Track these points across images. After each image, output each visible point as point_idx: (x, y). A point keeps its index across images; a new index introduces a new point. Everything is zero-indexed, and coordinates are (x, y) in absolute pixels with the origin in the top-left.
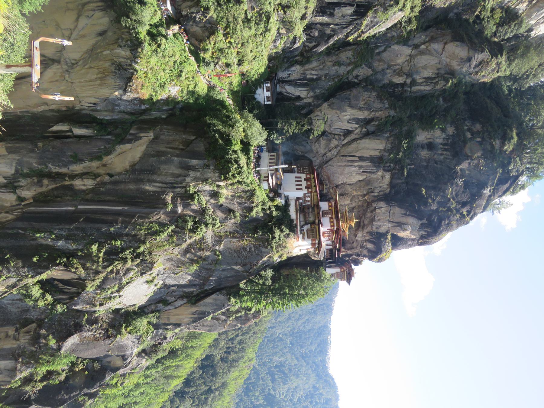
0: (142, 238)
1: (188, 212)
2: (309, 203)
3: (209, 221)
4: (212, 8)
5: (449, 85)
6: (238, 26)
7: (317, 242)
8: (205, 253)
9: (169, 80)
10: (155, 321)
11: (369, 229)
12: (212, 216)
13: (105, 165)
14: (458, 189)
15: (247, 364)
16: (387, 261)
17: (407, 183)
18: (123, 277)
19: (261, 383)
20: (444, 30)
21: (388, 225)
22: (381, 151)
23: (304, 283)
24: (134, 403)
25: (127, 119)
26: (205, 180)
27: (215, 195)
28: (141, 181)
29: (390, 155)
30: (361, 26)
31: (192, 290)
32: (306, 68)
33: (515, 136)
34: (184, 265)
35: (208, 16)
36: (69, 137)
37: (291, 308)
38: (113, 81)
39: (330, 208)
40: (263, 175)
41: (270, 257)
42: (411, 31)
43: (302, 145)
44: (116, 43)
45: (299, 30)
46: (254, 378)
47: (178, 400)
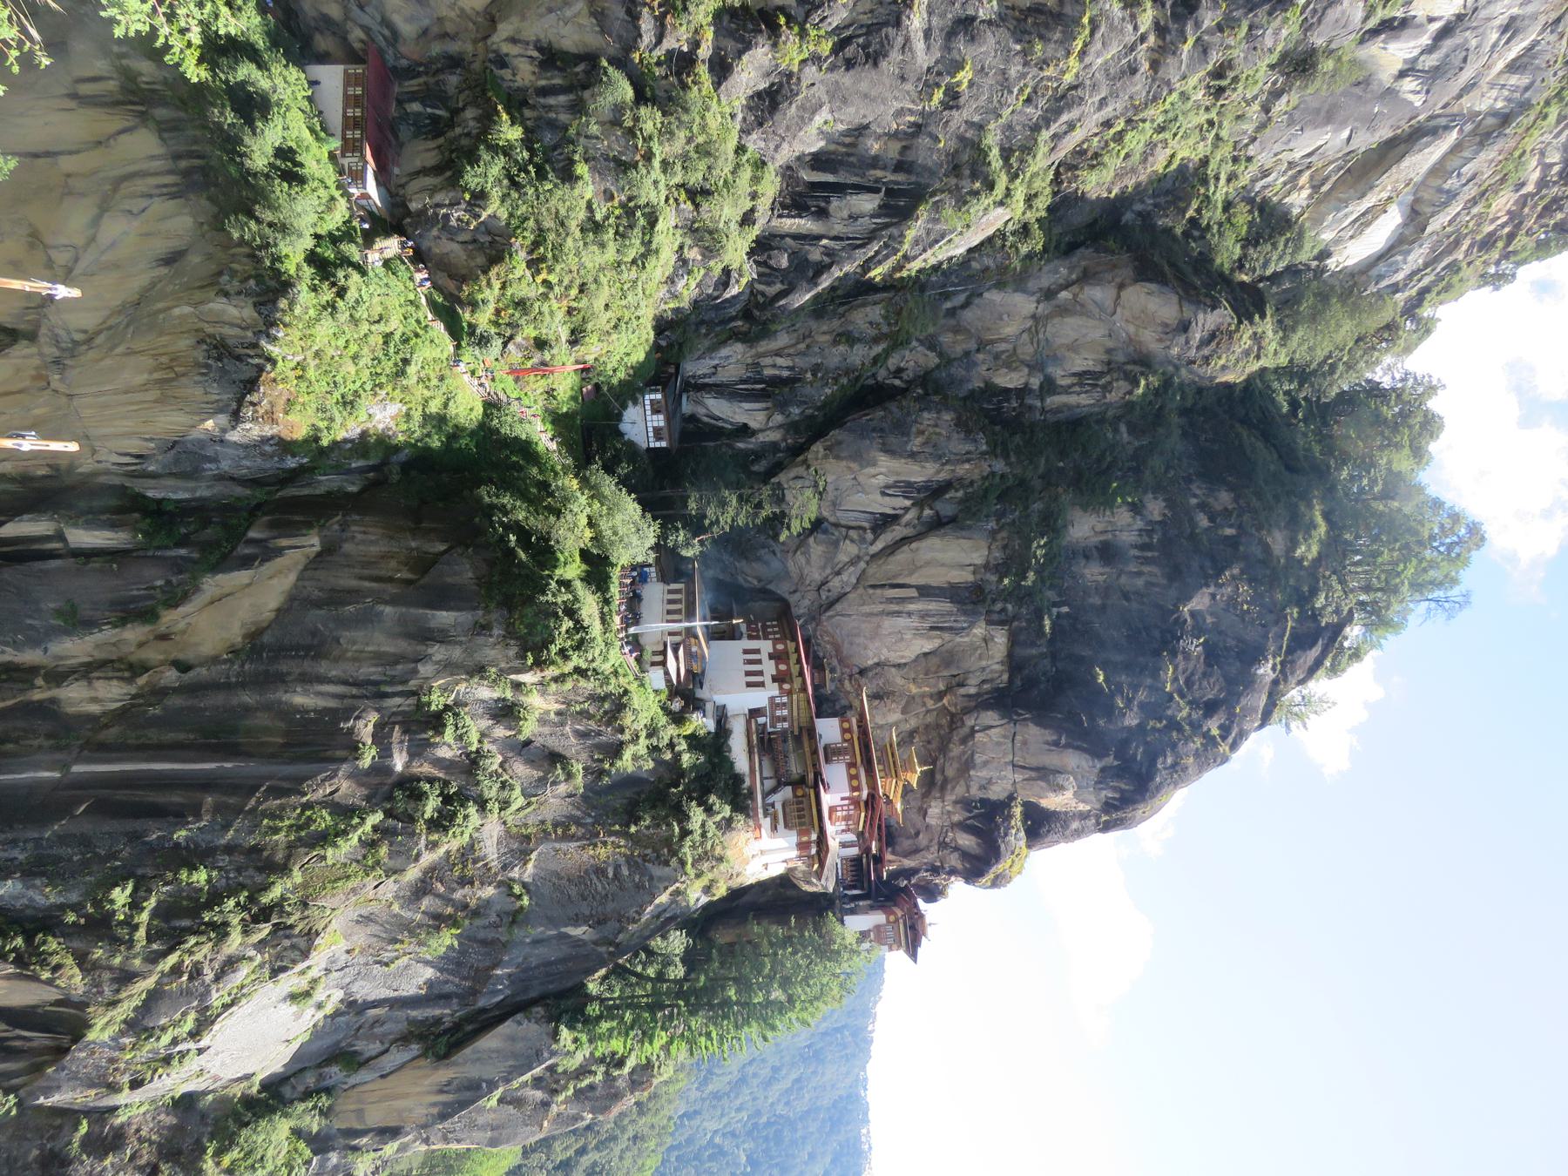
0: (280, 856)
1: (427, 769)
2: (786, 725)
3: (491, 791)
4: (495, 194)
5: (1141, 391)
6: (569, 241)
7: (814, 837)
8: (479, 893)
9: (368, 387)
10: (314, 1124)
11: (960, 790)
12: (499, 776)
13: (164, 637)
16: (1017, 880)
17: (1054, 656)
18: (214, 987)
20: (1113, 253)
22: (976, 569)
23: (783, 965)
25: (238, 499)
26: (479, 671)
27: (506, 712)
28: (281, 679)
29: (1001, 580)
30: (901, 243)
31: (437, 1012)
32: (760, 350)
33: (1319, 520)
34: (412, 933)
35: (484, 215)
36: (52, 555)
37: (746, 1048)
38: (199, 391)
39: (848, 736)
40: (649, 649)
41: (678, 892)
42: (1030, 256)
43: (759, 559)
44: (213, 283)
45: (736, 251)
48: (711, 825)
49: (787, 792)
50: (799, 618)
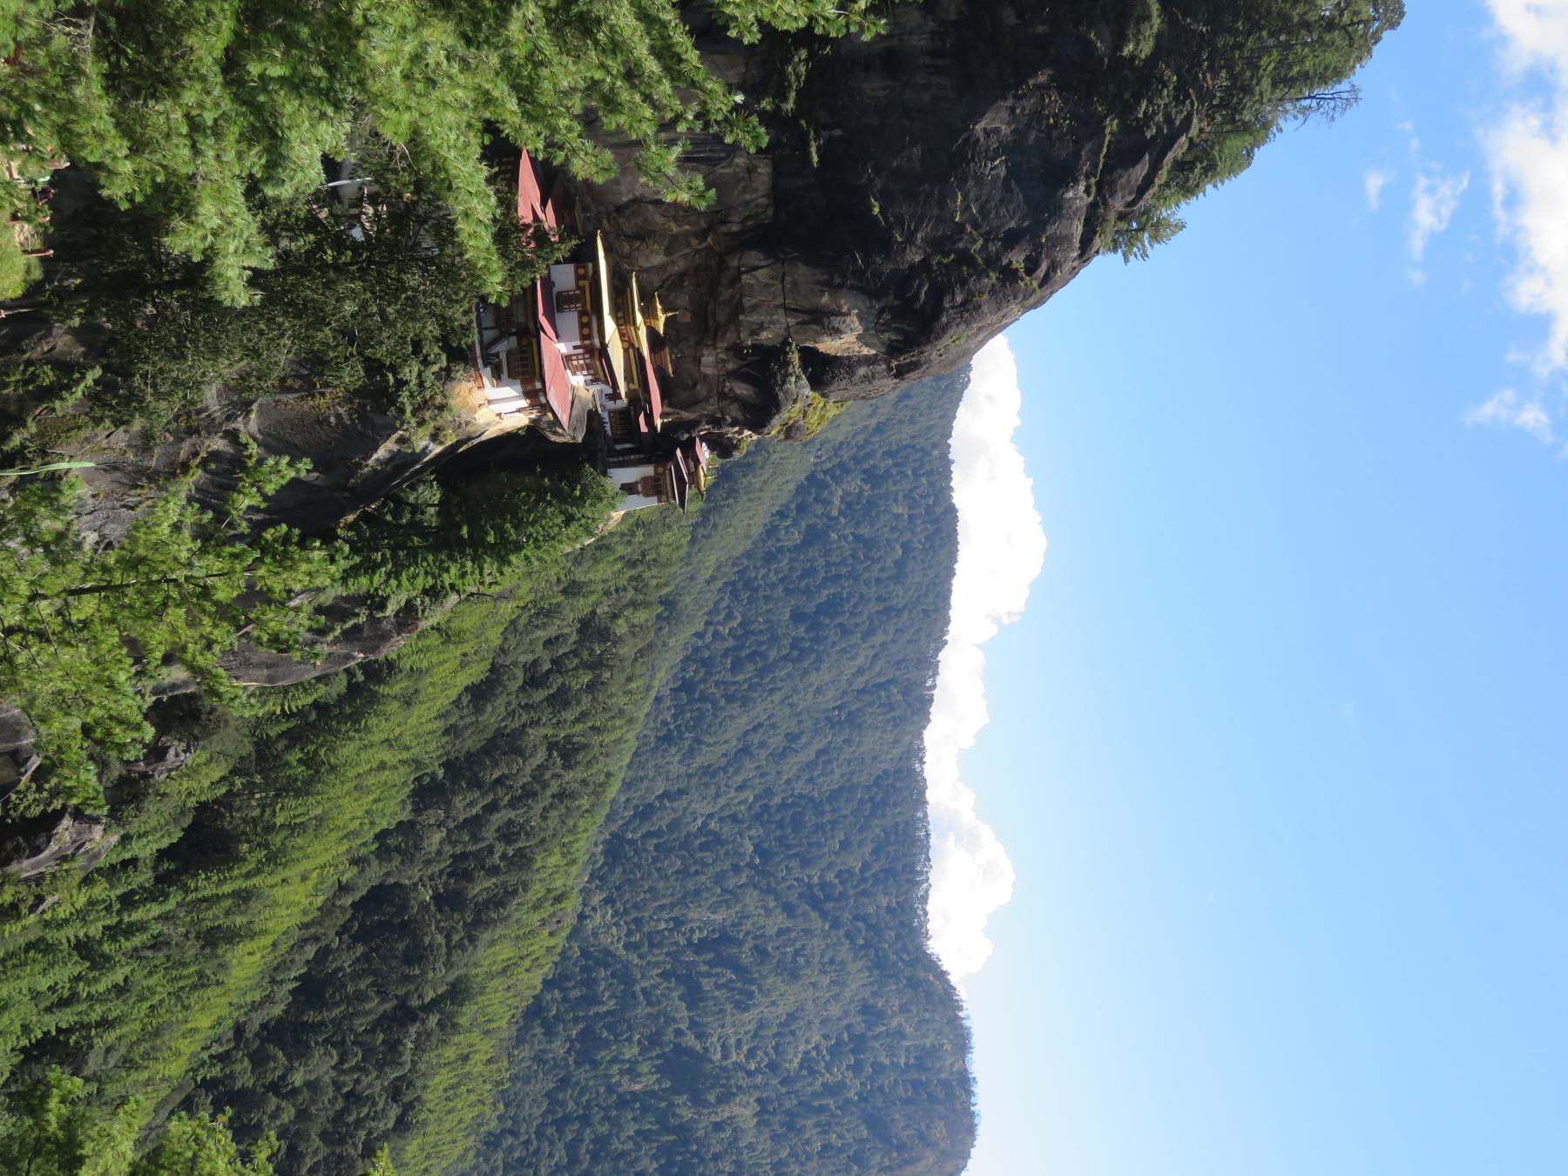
0: (13, 408)
7: (538, 385)
11: (730, 337)
14: (985, 190)
15: (544, 913)
19: (643, 1010)
21: (783, 319)
24: (98, 1025)
34: (151, 479)
39: (581, 283)
41: (401, 441)
46: (613, 996)
47: (280, 1054)
48: (429, 375)
49: (512, 342)
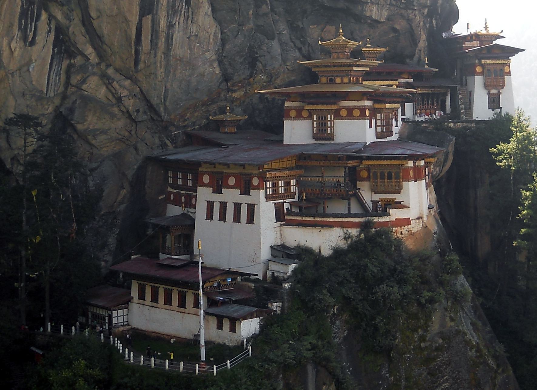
2: (293, 182)
7: (410, 164)
39: (305, 114)
50: (164, 146)
